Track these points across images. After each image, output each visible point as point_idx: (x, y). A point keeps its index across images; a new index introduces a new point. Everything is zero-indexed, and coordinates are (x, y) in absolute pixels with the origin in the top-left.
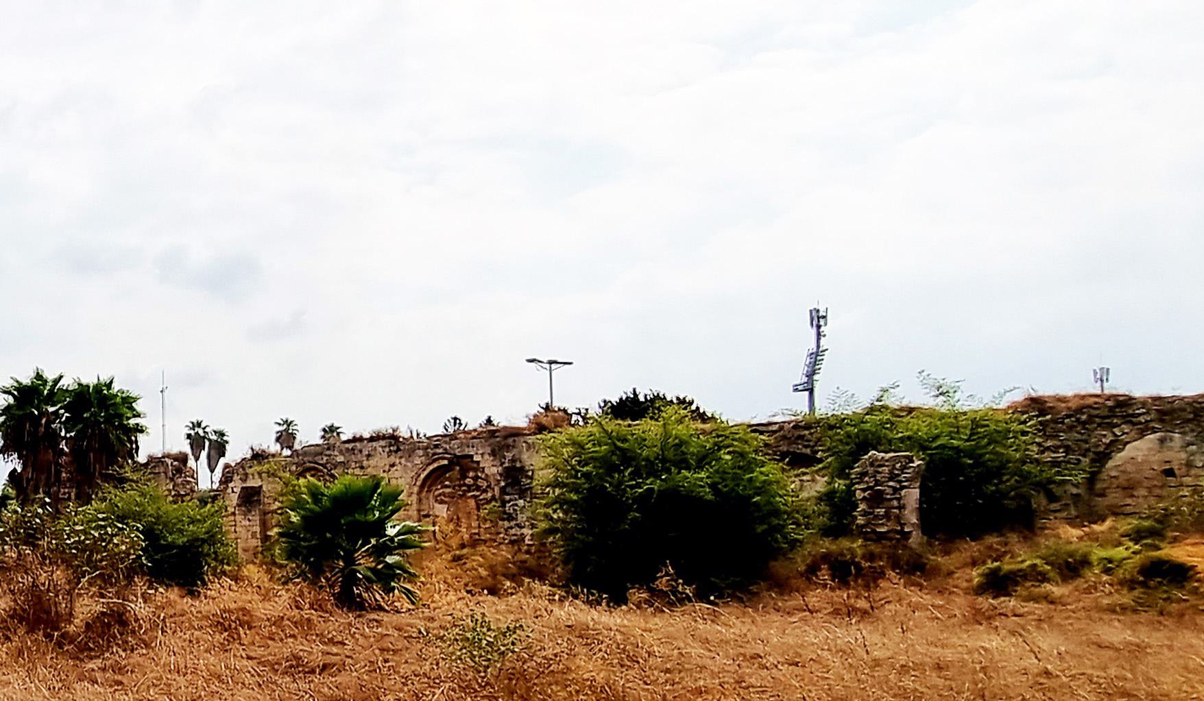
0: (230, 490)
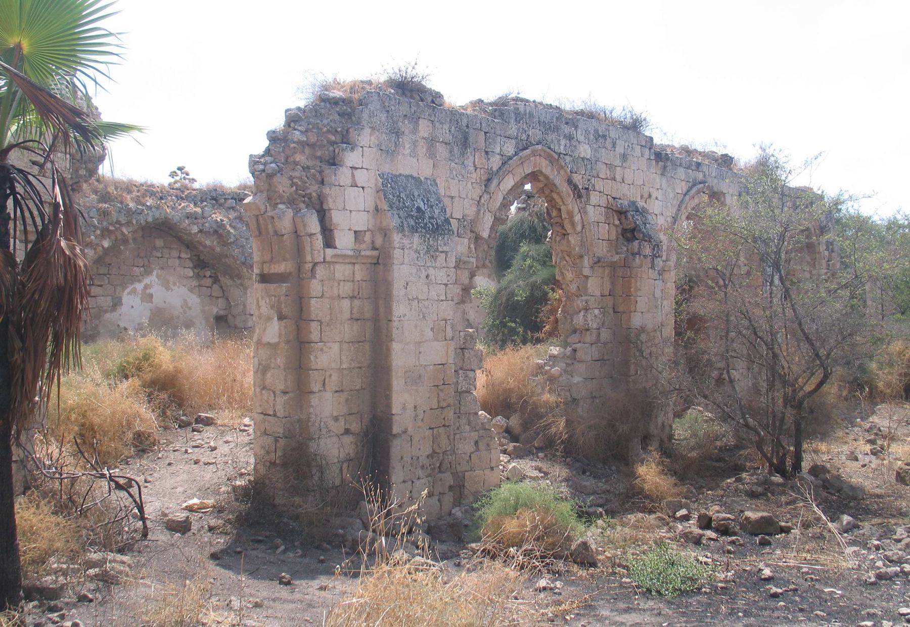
0: (343, 176)
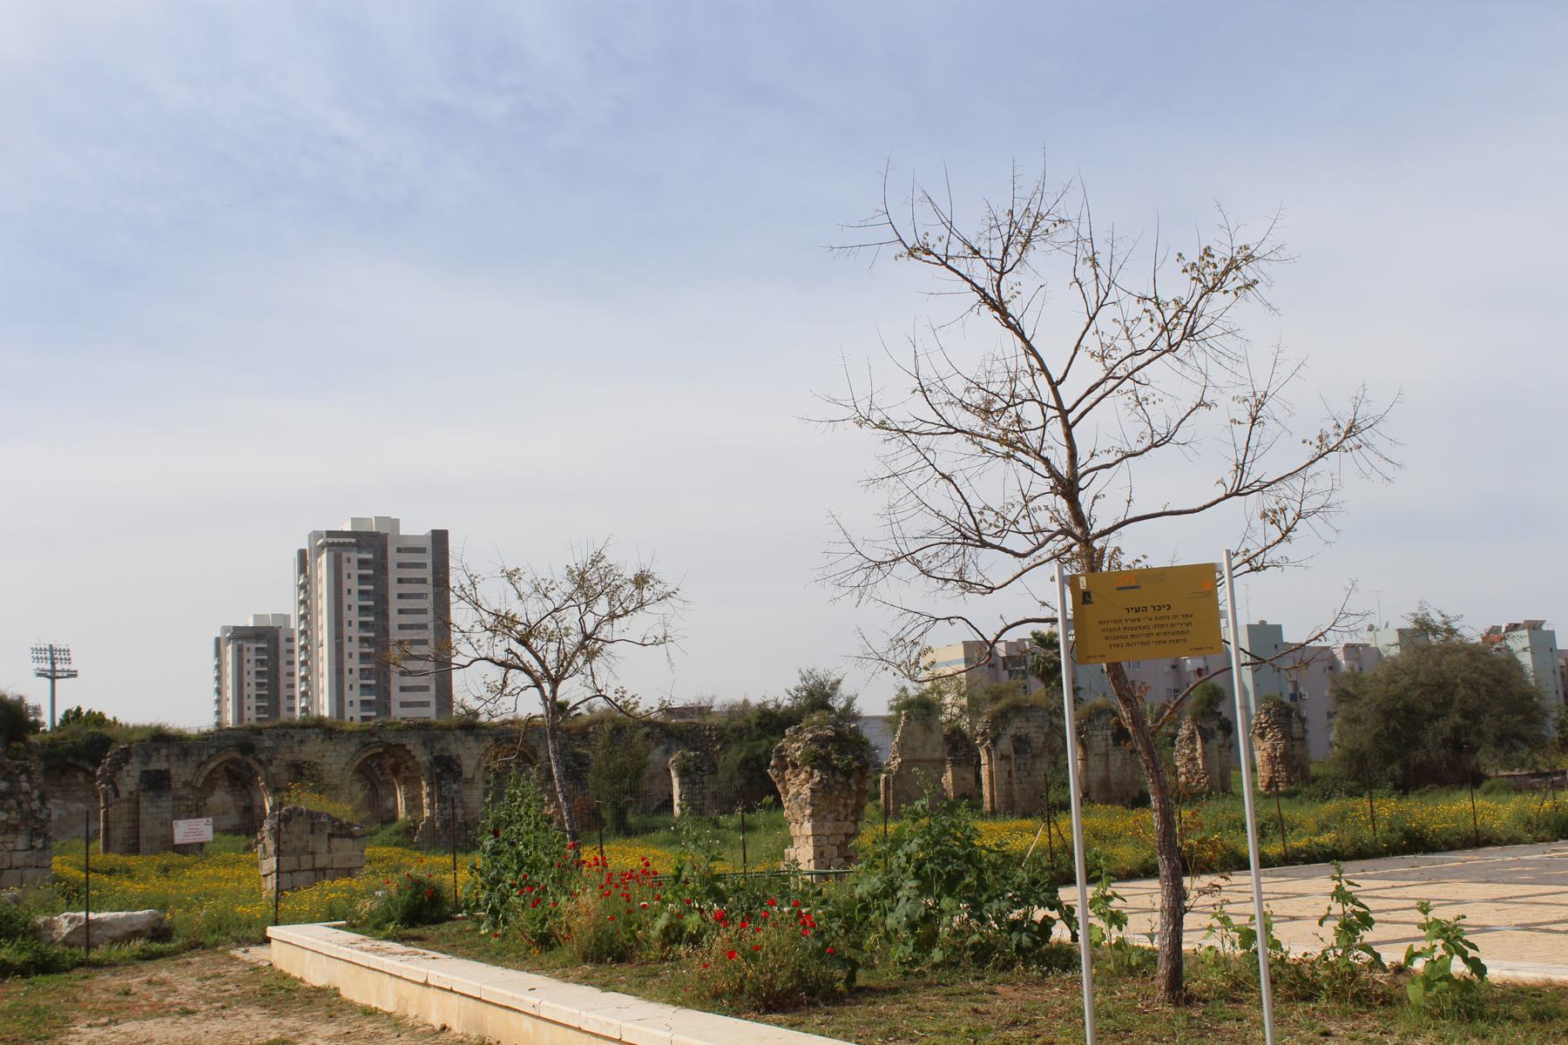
0: (124, 774)
